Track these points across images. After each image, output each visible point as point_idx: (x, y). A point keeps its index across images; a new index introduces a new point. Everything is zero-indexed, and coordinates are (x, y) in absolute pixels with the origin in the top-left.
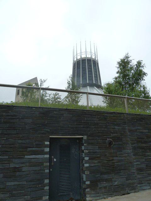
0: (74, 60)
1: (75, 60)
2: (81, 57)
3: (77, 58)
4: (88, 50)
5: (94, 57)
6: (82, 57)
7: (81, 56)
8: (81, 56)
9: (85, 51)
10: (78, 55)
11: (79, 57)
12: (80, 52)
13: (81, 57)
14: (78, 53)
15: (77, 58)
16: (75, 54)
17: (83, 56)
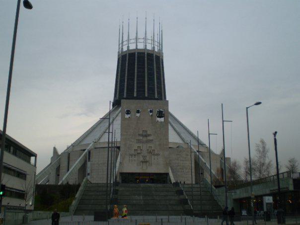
0: (122, 49)
1: (125, 49)
2: (137, 48)
3: (128, 47)
4: (149, 36)
5: (156, 50)
6: (139, 48)
7: (137, 45)
8: (137, 45)
9: (144, 36)
10: (132, 41)
11: (132, 47)
12: (134, 36)
13: (137, 48)
14: (130, 38)
15: (128, 47)
16: (125, 38)
17: (141, 46)
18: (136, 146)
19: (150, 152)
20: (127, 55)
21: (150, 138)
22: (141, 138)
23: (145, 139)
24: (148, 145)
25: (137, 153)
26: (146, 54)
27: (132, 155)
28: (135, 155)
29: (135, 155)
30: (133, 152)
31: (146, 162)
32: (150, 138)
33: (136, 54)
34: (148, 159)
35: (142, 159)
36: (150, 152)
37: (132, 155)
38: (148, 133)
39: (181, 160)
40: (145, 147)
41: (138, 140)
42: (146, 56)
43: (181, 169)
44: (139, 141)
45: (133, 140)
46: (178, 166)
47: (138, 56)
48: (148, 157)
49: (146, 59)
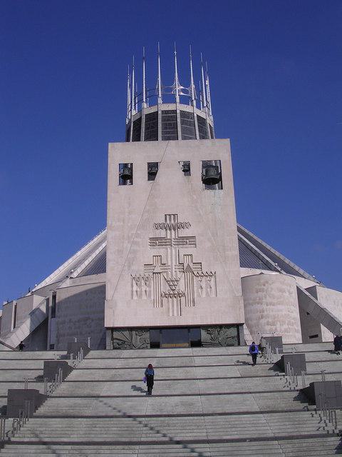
18: (148, 254)
19: (189, 269)
20: (144, 117)
21: (184, 233)
22: (162, 233)
23: (171, 235)
24: (185, 250)
25: (154, 271)
26: (178, 112)
27: (136, 279)
28: (147, 280)
29: (147, 280)
30: (139, 269)
31: (180, 295)
32: (184, 233)
33: (160, 112)
34: (181, 287)
35: (165, 288)
36: (189, 269)
37: (136, 279)
38: (180, 220)
39: (267, 305)
40: (170, 255)
41: (157, 239)
42: (179, 116)
43: (268, 324)
44: (155, 241)
45: (139, 240)
46: (262, 318)
47: (163, 117)
48: (182, 281)
49: (179, 120)
